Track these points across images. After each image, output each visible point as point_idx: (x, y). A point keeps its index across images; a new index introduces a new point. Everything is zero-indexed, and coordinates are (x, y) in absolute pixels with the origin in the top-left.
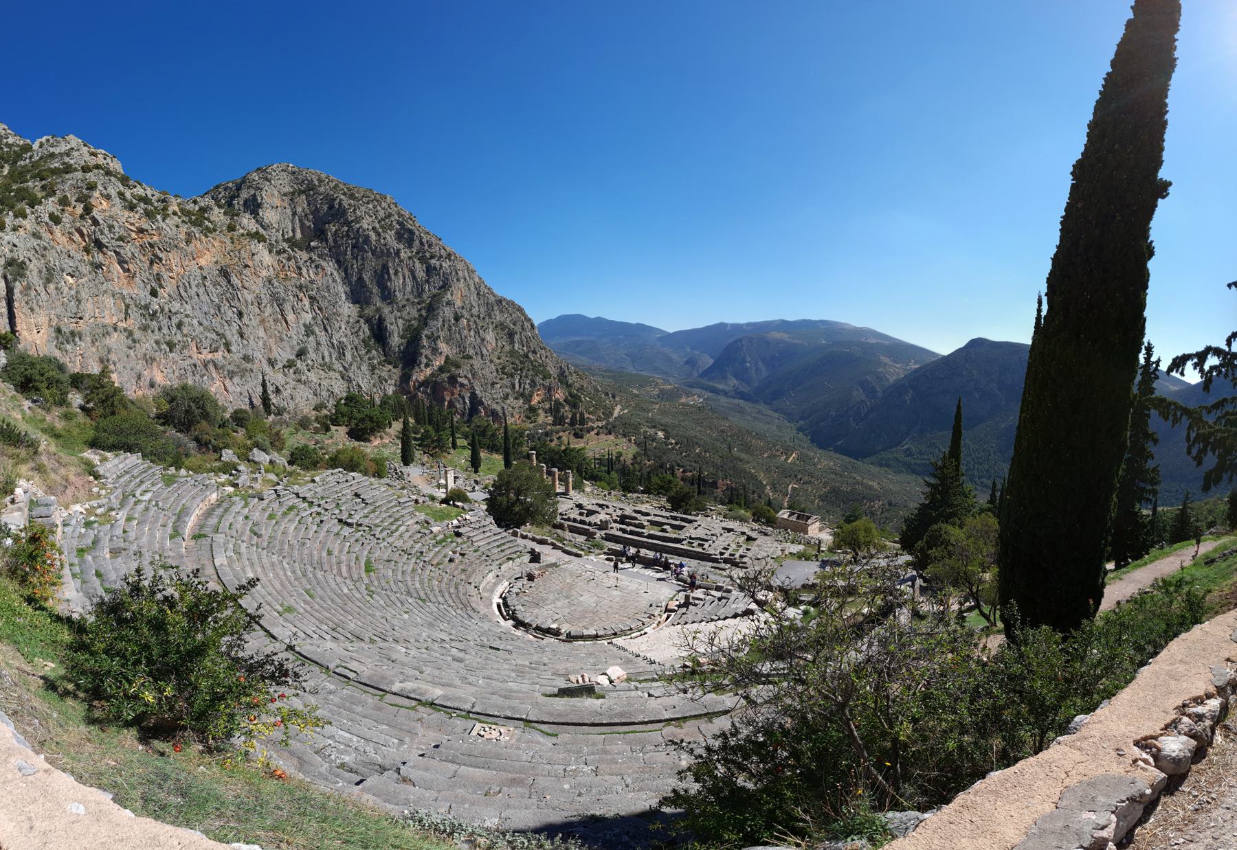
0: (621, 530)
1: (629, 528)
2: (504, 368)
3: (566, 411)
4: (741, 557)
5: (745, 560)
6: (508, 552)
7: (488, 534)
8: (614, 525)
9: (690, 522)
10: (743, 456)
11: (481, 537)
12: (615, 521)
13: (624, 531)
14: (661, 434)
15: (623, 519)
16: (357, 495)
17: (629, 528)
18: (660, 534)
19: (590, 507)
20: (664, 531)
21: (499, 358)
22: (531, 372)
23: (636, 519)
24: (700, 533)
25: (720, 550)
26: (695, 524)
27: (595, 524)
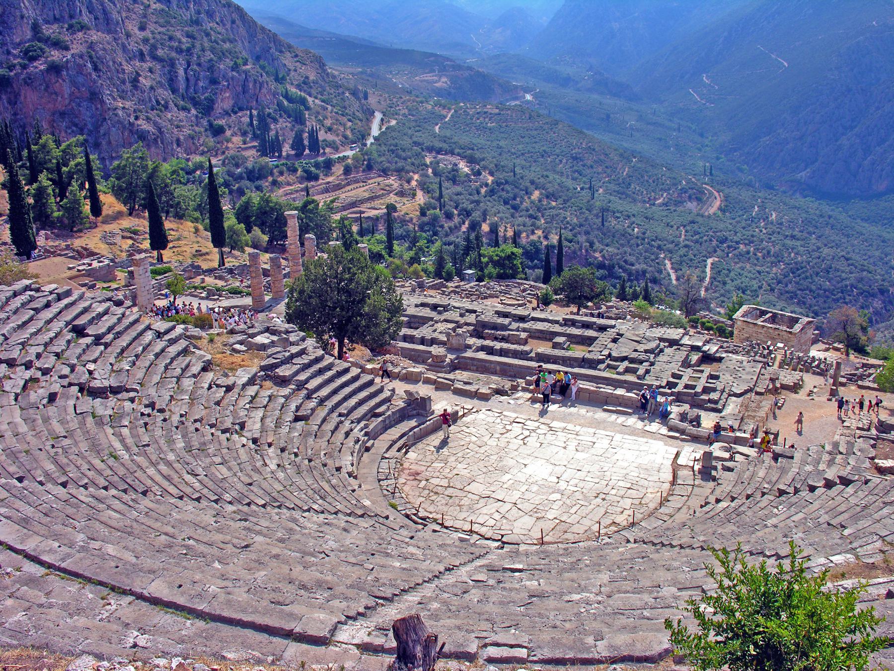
0: (482, 348)
1: (498, 345)
2: (154, 47)
3: (282, 127)
4: (706, 390)
5: (714, 396)
6: (372, 403)
7: (329, 374)
8: (471, 341)
9: (603, 329)
10: (618, 204)
11: (318, 380)
12: (471, 336)
13: (490, 351)
14: (464, 167)
15: (479, 330)
16: (80, 332)
17: (498, 345)
18: (558, 352)
19: (411, 311)
20: (556, 346)
21: (142, 28)
22: (209, 55)
23: (504, 328)
24: (623, 349)
25: (666, 378)
26: (612, 333)
27: (433, 342)
